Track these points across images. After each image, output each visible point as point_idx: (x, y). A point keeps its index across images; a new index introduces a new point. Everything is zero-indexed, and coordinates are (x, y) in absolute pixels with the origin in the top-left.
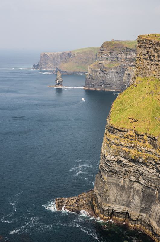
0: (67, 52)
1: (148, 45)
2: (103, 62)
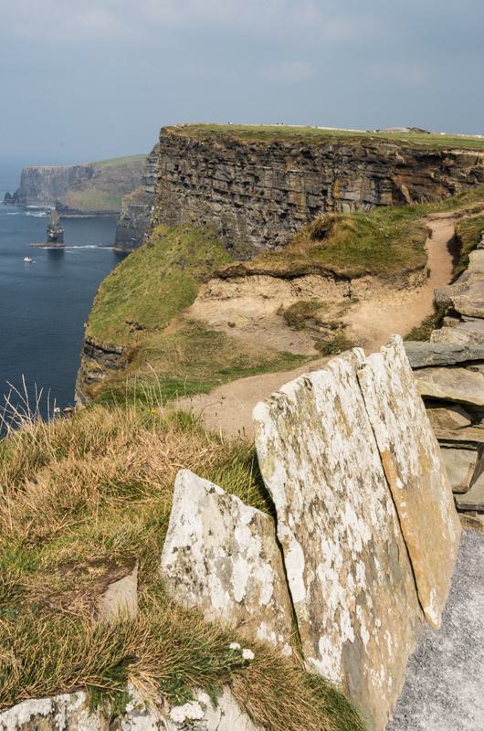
1: (176, 150)
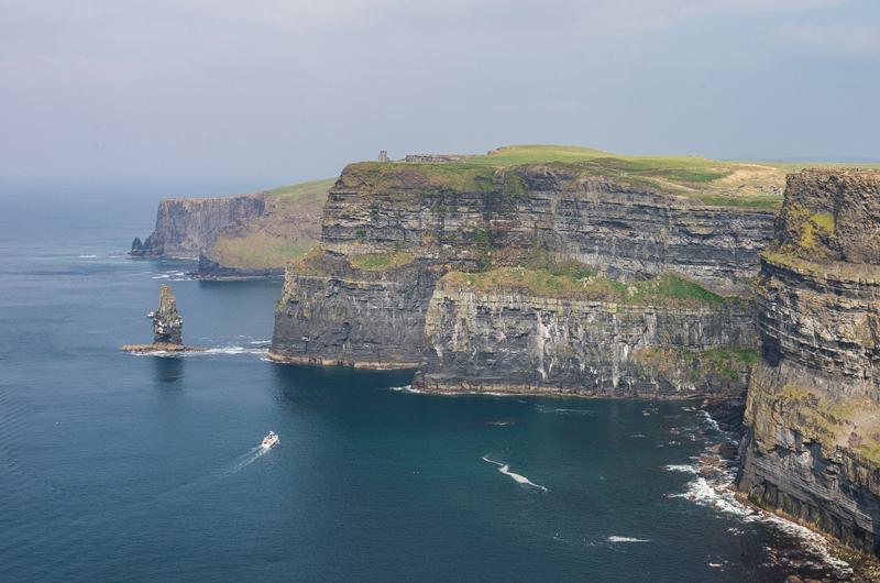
0: (253, 194)
2: (345, 246)
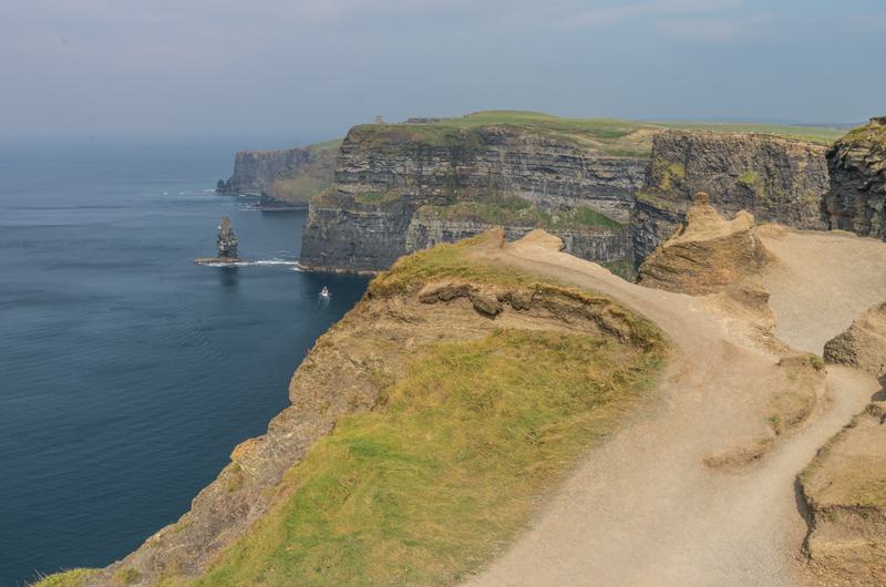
0: (302, 147)
2: (351, 186)
